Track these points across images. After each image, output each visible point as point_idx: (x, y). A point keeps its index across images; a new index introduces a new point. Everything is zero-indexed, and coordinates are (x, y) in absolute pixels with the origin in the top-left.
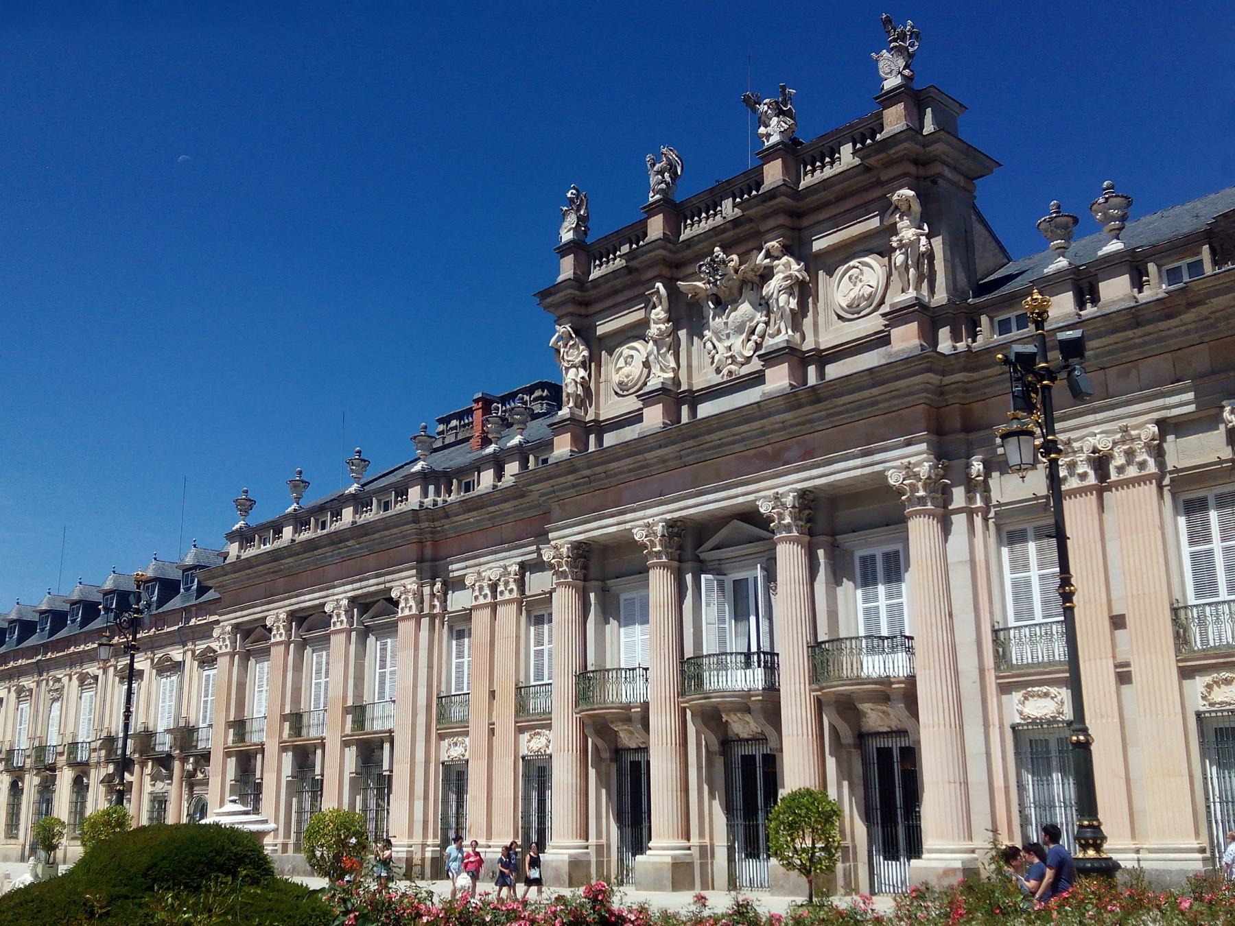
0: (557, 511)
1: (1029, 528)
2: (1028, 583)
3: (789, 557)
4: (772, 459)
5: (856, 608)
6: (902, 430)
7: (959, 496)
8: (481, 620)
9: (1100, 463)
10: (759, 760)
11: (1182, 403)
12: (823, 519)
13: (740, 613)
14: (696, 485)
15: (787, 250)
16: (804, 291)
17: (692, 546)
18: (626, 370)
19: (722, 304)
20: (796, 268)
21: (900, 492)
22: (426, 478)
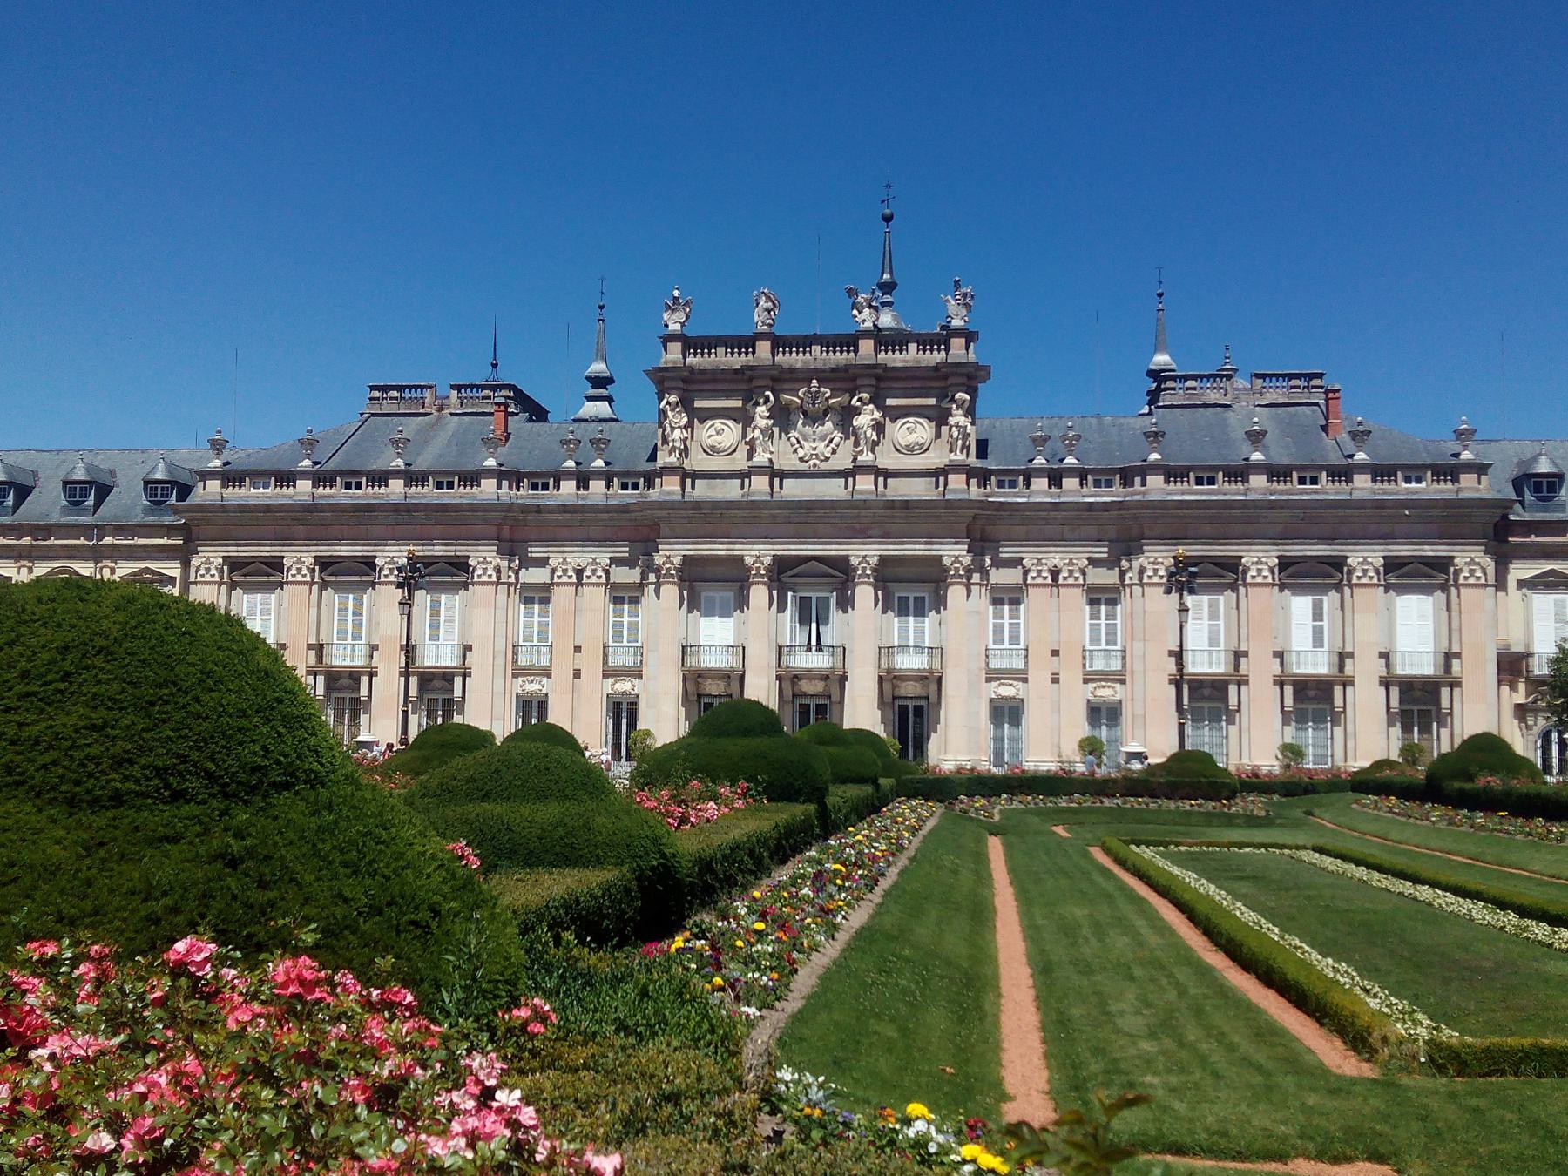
0: (665, 529)
1: (1006, 597)
2: (1002, 625)
3: (864, 594)
4: (862, 533)
5: (896, 627)
6: (954, 537)
7: (976, 578)
8: (562, 596)
9: (1055, 573)
10: (813, 709)
11: (1101, 552)
12: (888, 576)
13: (804, 620)
14: (799, 537)
15: (871, 401)
16: (879, 428)
17: (782, 574)
18: (719, 438)
19: (814, 419)
20: (877, 415)
21: (947, 570)
22: (500, 474)
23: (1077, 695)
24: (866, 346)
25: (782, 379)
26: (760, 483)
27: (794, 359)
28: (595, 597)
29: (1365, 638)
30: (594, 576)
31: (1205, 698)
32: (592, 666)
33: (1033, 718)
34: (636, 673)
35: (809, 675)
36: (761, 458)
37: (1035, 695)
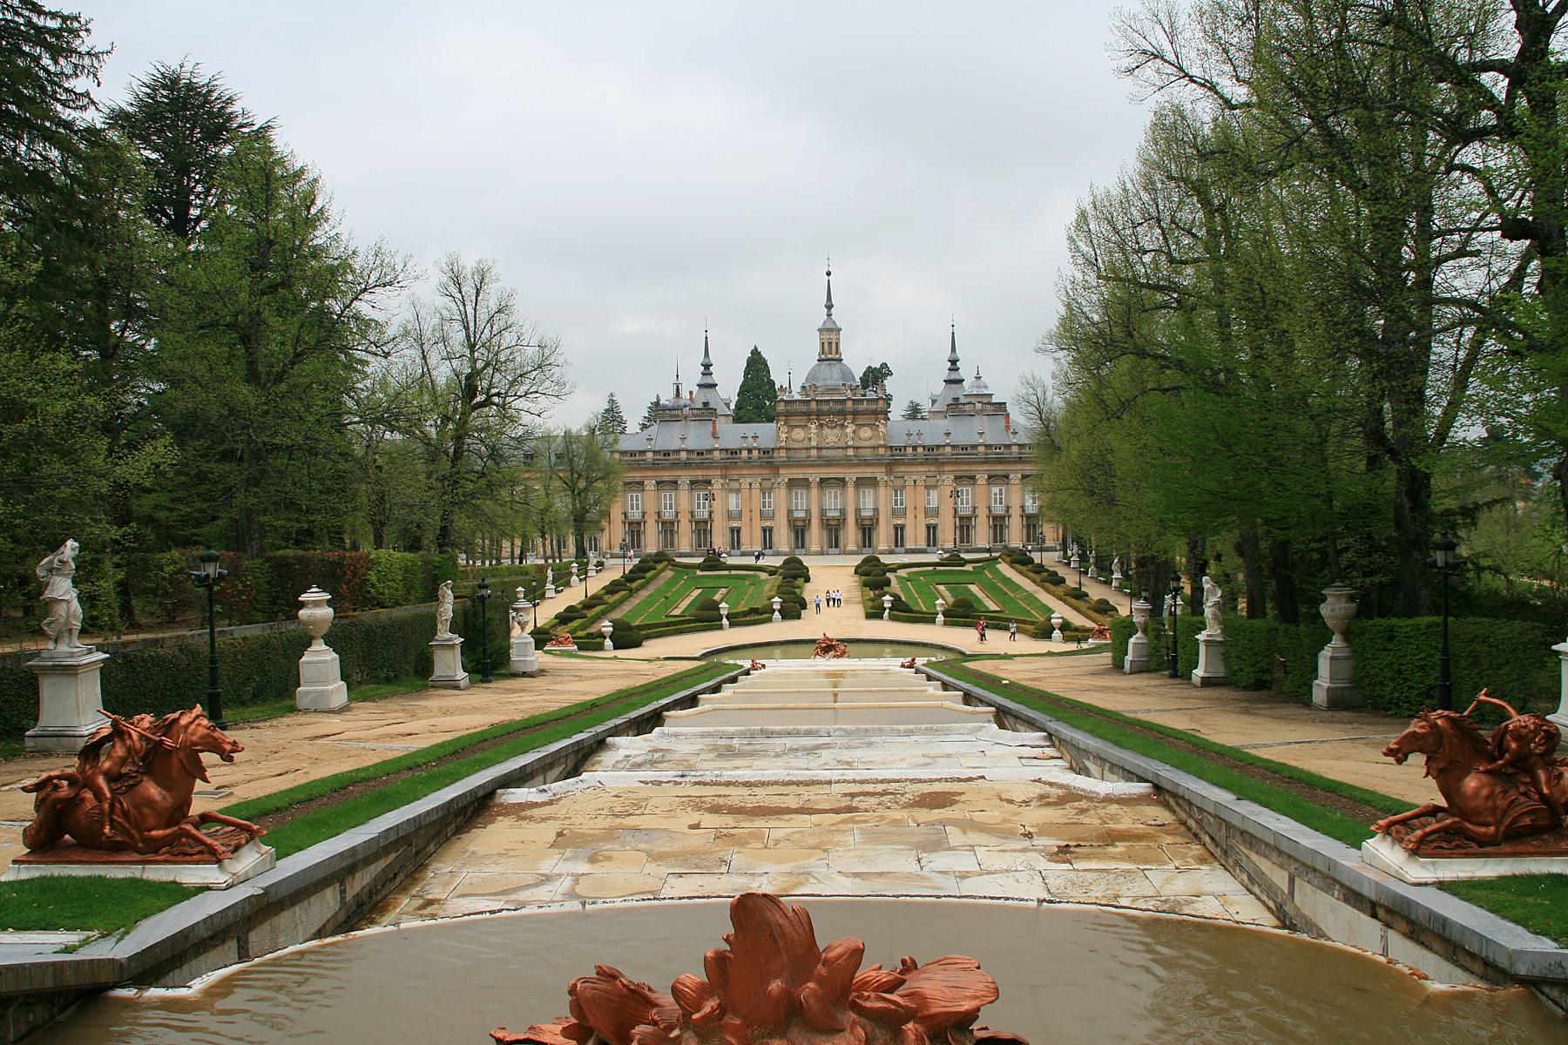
8: (745, 492)
23: (922, 522)
24: (849, 404)
25: (819, 414)
26: (814, 452)
27: (825, 408)
28: (756, 493)
29: (1015, 502)
30: (756, 485)
31: (965, 526)
32: (756, 517)
33: (908, 533)
34: (772, 518)
35: (833, 518)
36: (814, 443)
37: (908, 521)
